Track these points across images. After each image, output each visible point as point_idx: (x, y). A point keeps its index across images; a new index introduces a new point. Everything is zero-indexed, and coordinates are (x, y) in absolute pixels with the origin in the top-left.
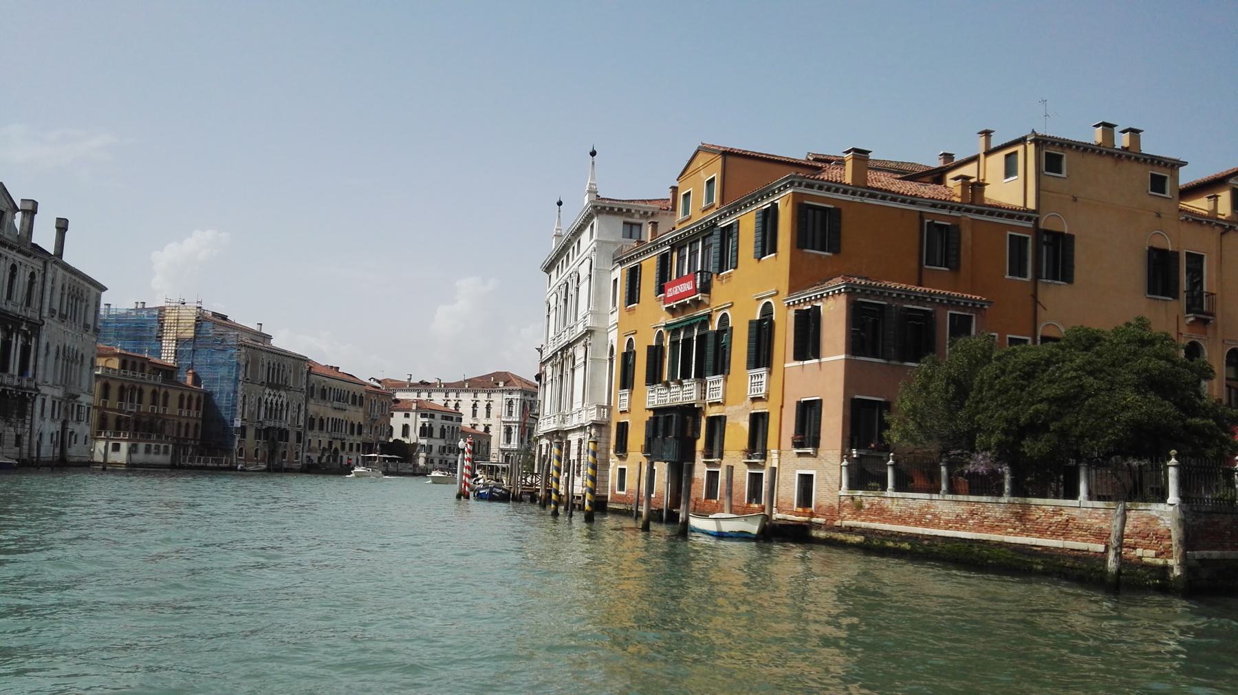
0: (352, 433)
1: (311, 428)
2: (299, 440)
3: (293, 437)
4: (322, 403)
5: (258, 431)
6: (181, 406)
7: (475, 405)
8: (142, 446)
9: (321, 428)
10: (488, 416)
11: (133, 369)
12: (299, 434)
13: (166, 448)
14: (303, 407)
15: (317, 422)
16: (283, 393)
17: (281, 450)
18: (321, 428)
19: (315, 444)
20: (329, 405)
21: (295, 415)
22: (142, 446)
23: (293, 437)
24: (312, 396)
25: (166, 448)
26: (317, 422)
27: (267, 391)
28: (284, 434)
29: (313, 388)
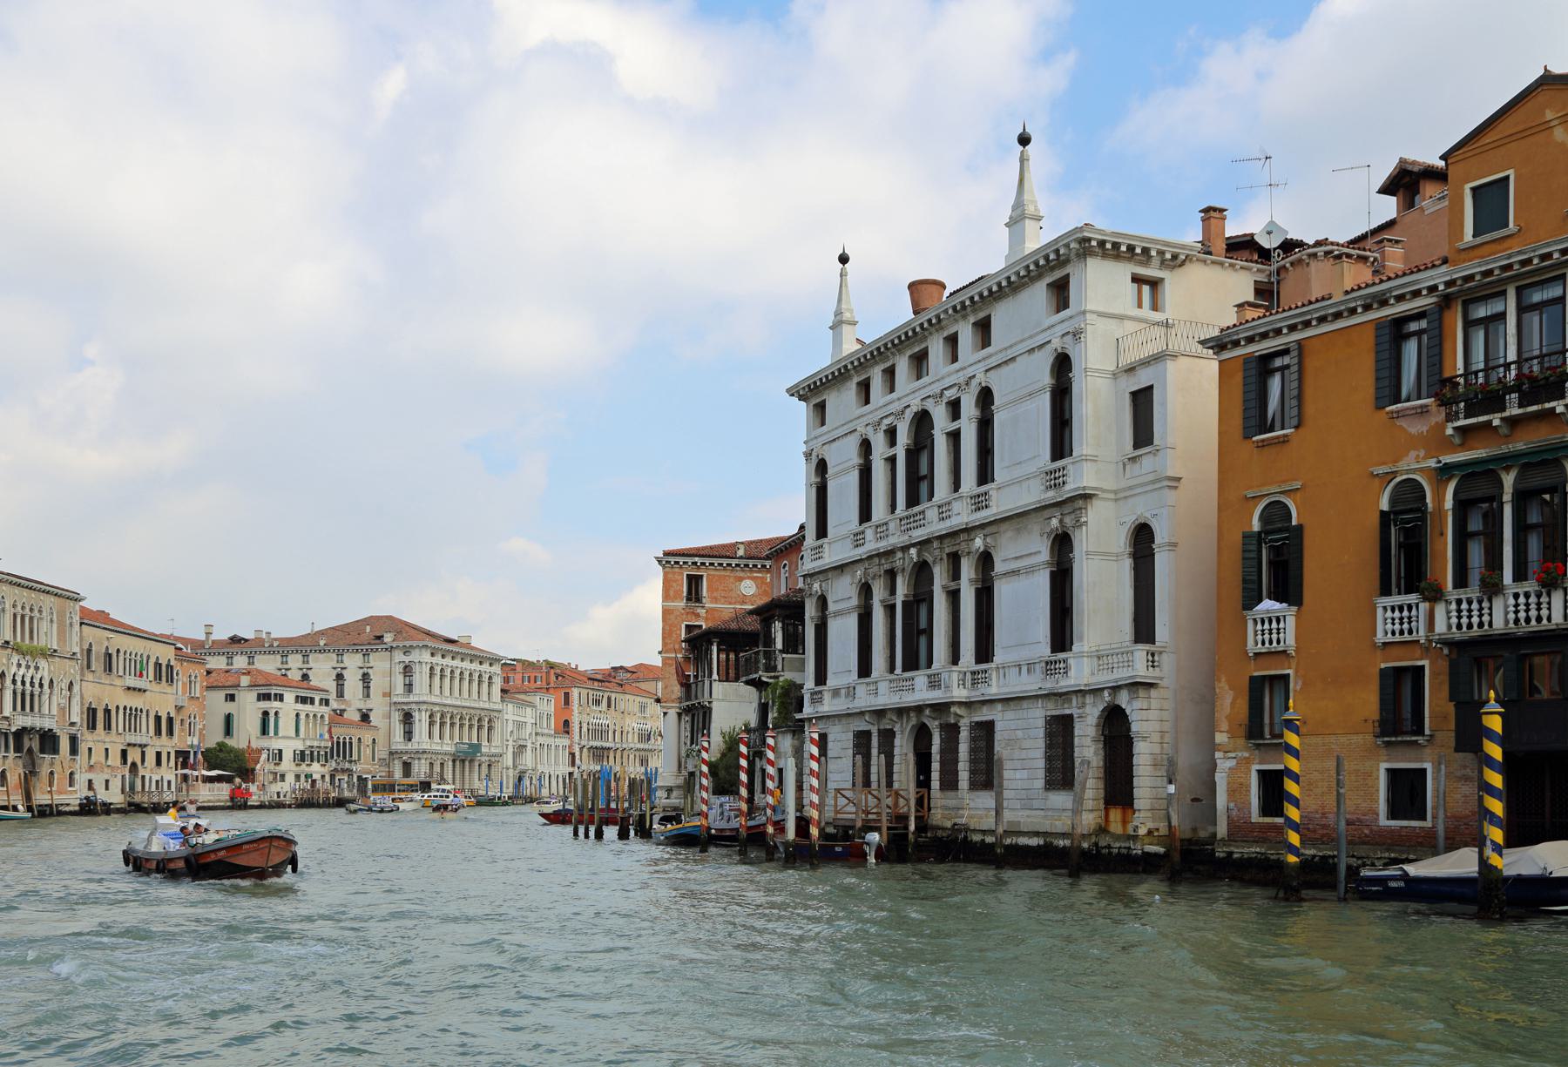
0: (158, 732)
1: (92, 726)
2: (74, 751)
3: (64, 745)
4: (105, 679)
7: (340, 677)
9: (108, 727)
12: (73, 740)
14: (76, 688)
15: (100, 715)
16: (43, 663)
17: (44, 771)
18: (108, 727)
19: (98, 756)
20: (118, 682)
21: (64, 702)
23: (64, 745)
24: (89, 667)
26: (100, 715)
27: (15, 658)
29: (89, 651)
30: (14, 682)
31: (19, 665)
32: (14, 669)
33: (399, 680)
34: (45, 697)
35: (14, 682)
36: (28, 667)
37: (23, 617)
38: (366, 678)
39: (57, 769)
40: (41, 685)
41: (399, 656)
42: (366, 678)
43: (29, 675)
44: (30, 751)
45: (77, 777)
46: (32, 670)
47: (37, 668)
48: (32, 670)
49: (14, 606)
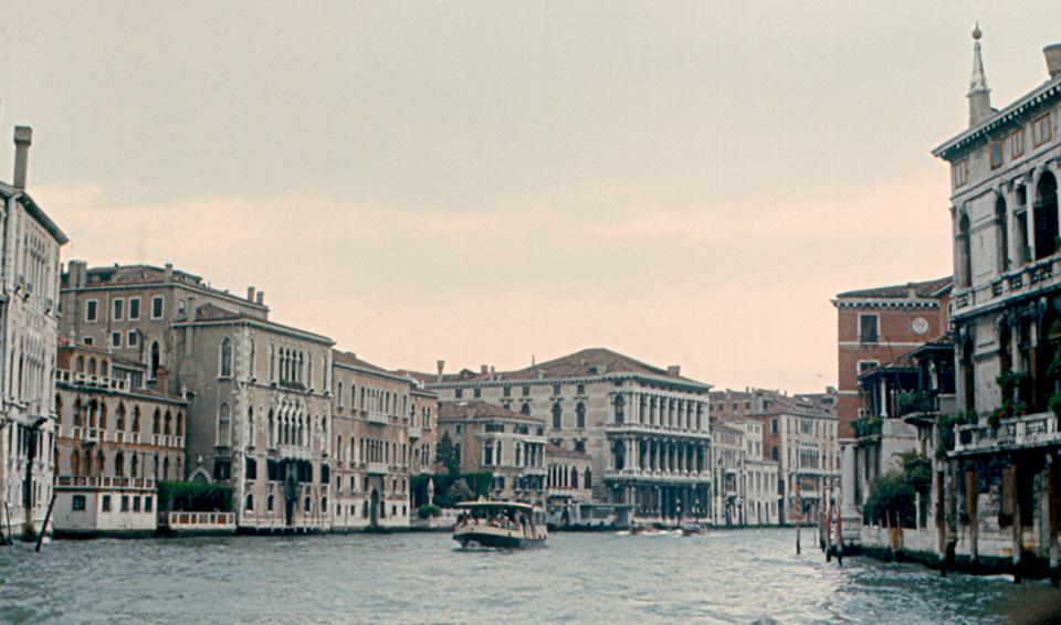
2: (325, 479)
5: (272, 466)
6: (156, 429)
8: (116, 499)
10: (581, 423)
11: (93, 370)
13: (149, 501)
22: (116, 499)
25: (149, 501)
28: (304, 469)
30: (280, 418)
31: (284, 404)
32: (279, 407)
33: (611, 411)
34: (305, 432)
35: (280, 418)
36: (291, 405)
37: (288, 361)
38: (580, 408)
39: (312, 496)
40: (300, 421)
41: (610, 387)
42: (580, 408)
43: (291, 412)
44: (291, 478)
45: (328, 502)
46: (293, 408)
47: (298, 406)
48: (293, 408)
49: (281, 352)
